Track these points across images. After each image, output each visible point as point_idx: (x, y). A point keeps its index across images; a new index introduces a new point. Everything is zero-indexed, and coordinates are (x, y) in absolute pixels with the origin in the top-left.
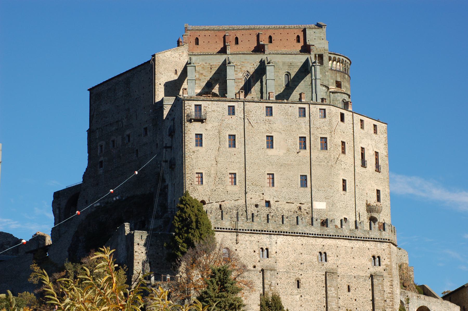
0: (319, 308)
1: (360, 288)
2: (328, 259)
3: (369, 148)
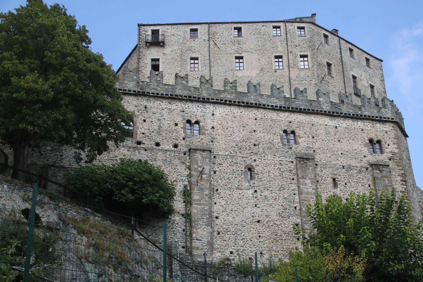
0: (287, 211)
1: (352, 183)
2: (300, 140)
3: (362, 78)
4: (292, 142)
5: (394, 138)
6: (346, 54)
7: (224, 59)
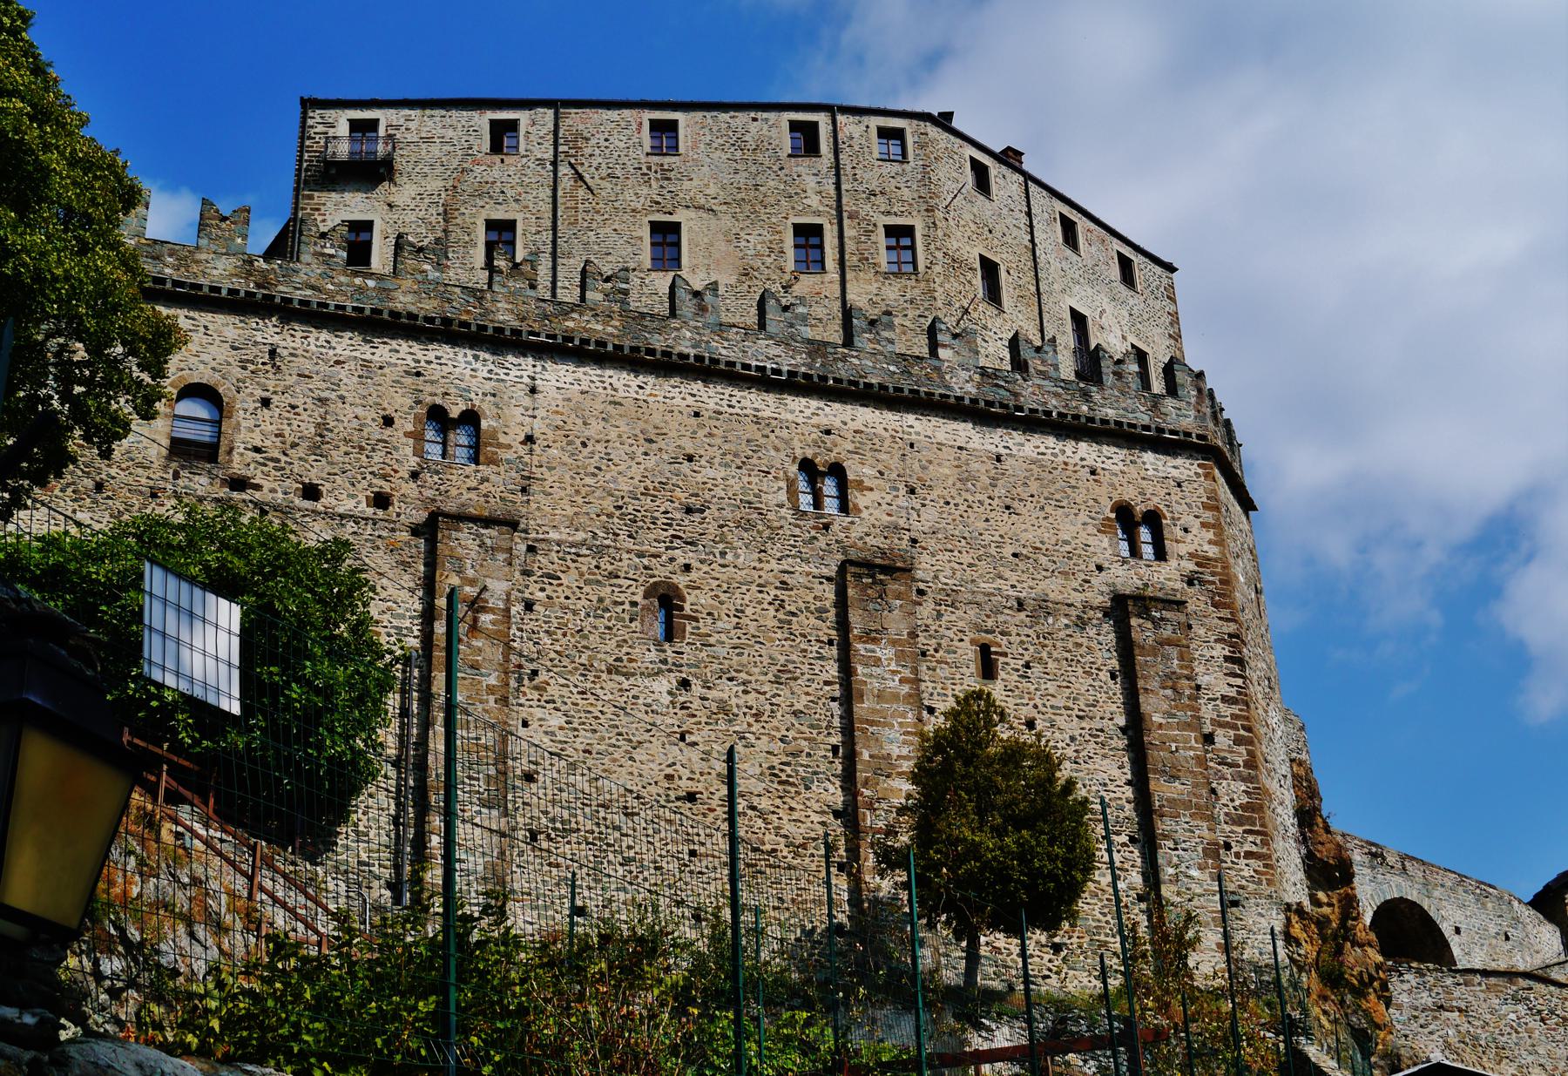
0: (803, 760)
1: (1051, 665)
4: (831, 506)
5: (1205, 507)
6: (1049, 236)
7: (608, 230)
